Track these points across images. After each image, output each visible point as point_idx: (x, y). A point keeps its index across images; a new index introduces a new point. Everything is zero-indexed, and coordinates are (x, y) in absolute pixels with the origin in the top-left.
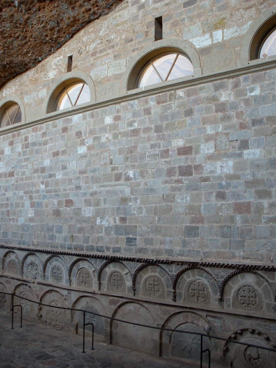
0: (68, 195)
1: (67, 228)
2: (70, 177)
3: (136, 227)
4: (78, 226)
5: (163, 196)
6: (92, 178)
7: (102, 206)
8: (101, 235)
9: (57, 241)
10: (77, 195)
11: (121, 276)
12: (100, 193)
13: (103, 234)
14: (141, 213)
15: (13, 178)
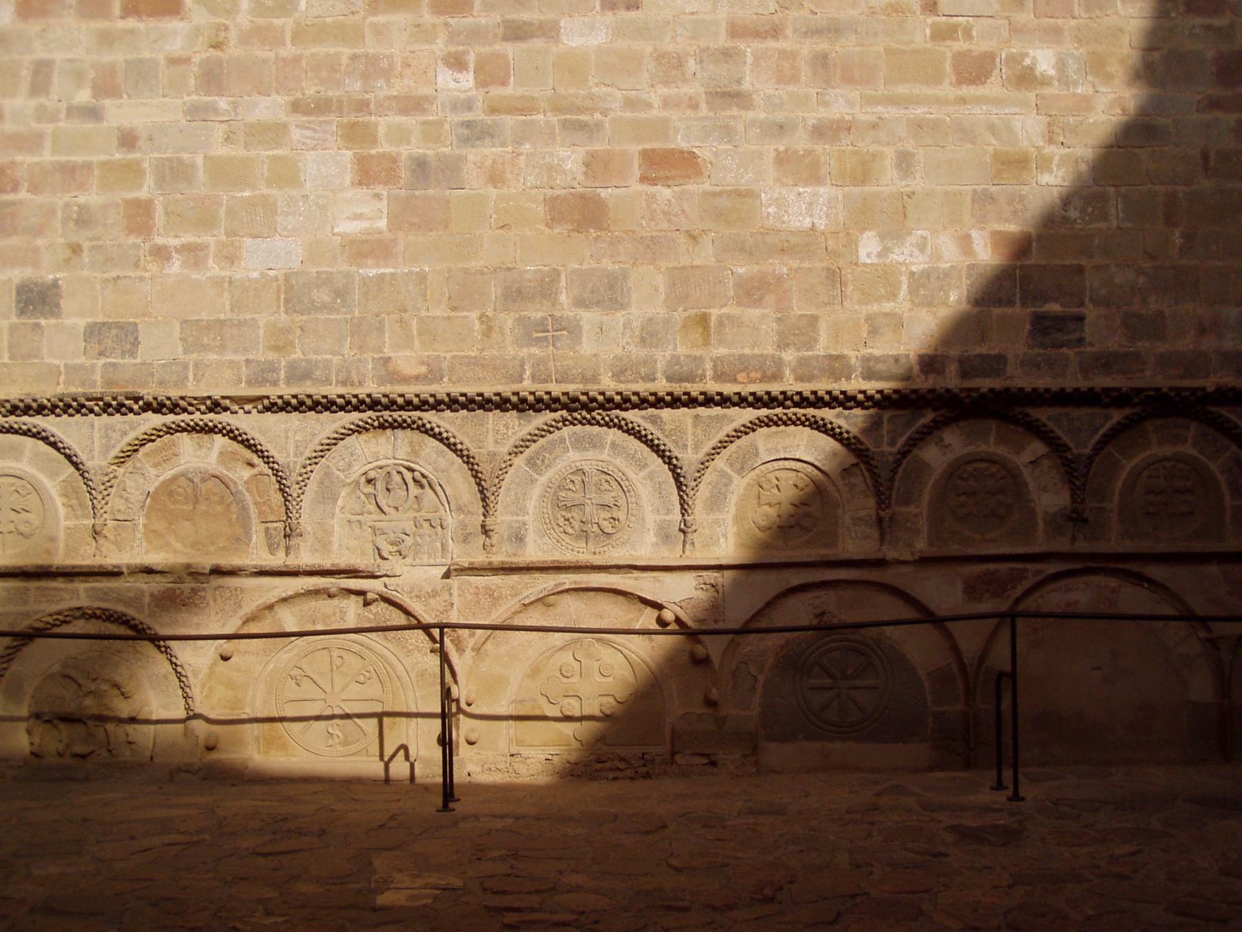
0: (662, 128)
1: (661, 280)
2: (670, 48)
3: (1080, 270)
4: (741, 270)
5: (1205, 156)
6: (821, 61)
7: (889, 181)
8: (888, 306)
9: (587, 347)
10: (727, 132)
11: (1012, 474)
12: (874, 126)
13: (902, 303)
14: (1104, 217)
15: (173, 24)
